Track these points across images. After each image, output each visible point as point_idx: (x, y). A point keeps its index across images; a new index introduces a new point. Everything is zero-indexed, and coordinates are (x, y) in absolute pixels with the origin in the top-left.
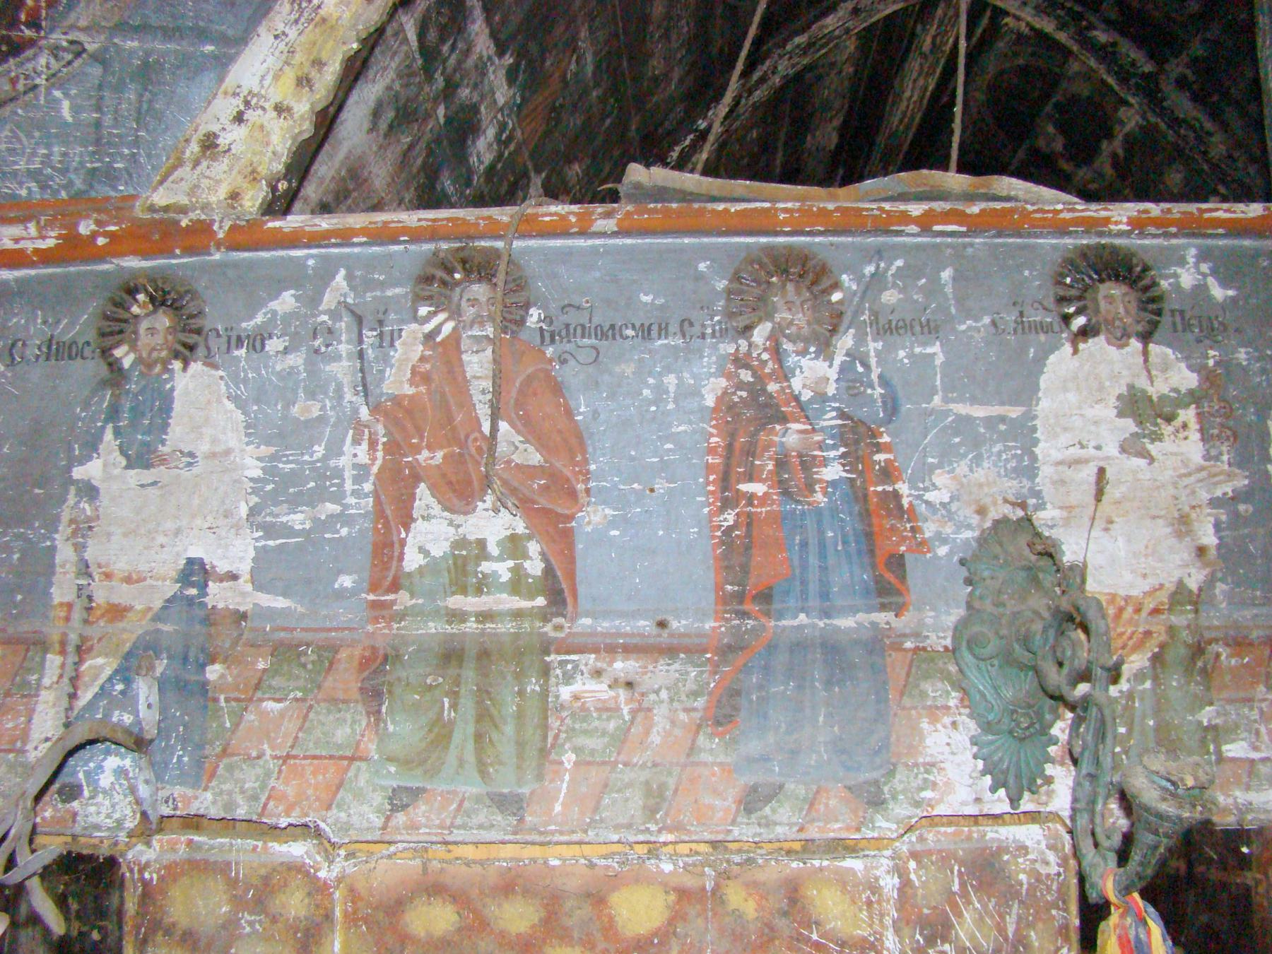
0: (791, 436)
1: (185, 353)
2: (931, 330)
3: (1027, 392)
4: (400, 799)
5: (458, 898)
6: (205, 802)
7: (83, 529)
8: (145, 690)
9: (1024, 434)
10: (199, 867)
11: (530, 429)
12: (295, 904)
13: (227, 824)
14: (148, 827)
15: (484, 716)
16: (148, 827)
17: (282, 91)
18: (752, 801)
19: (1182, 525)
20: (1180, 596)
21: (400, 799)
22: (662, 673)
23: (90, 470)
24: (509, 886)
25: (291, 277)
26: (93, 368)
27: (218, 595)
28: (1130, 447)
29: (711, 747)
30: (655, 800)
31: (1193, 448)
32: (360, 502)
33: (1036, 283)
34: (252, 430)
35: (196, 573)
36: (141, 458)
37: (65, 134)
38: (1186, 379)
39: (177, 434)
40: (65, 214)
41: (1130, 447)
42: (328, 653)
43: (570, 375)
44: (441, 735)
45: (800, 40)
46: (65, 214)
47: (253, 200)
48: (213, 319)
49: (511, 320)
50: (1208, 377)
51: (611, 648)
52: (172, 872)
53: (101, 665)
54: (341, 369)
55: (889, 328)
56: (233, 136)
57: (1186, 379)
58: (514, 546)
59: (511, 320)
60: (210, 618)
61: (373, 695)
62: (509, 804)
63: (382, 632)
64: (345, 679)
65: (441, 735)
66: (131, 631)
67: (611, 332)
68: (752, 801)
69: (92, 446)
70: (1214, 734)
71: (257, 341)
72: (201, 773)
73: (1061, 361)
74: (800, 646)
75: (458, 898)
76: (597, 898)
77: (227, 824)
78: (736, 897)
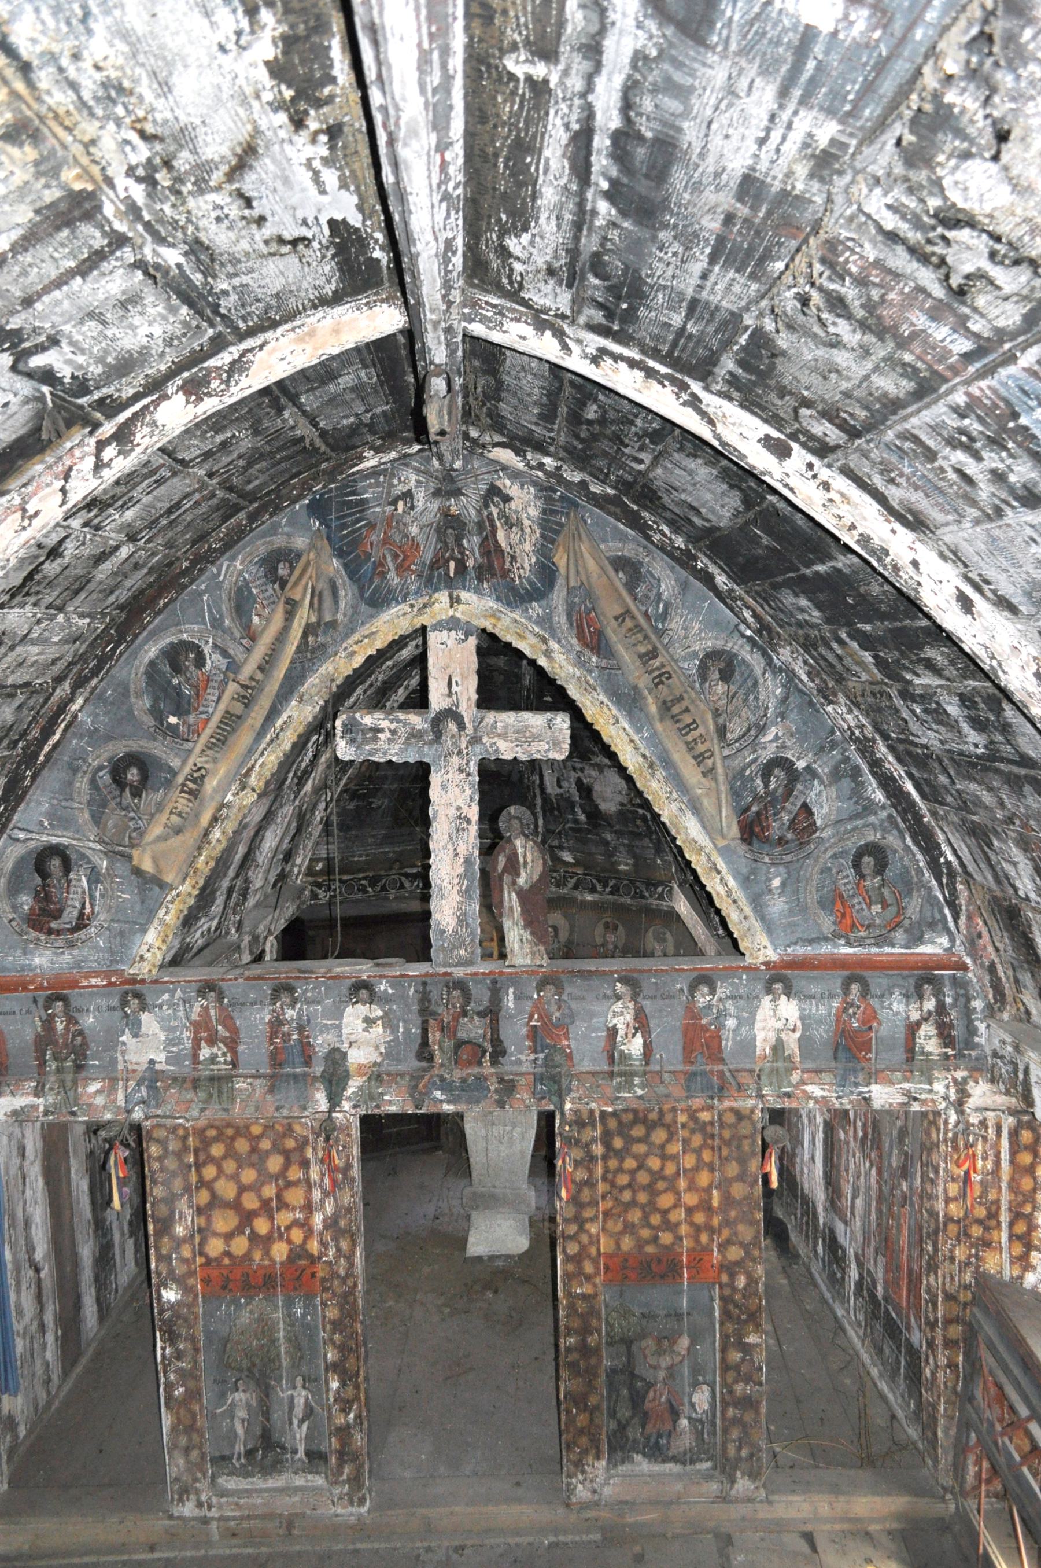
0: (285, 1028)
1: (143, 1010)
2: (318, 1003)
3: (340, 1017)
4: (202, 1110)
5: (217, 1128)
6: (159, 1112)
7: (123, 1052)
8: (143, 1089)
9: (339, 1027)
10: (159, 1126)
11: (225, 1026)
12: (181, 1132)
13: (164, 1117)
14: (147, 1118)
15: (220, 1092)
16: (147, 1118)
17: (158, 944)
18: (278, 1109)
19: (377, 1048)
20: (375, 1064)
21: (202, 1110)
22: (258, 1082)
23: (123, 1038)
24: (228, 1125)
25: (168, 991)
26: (118, 1014)
27: (158, 1067)
28: (365, 1030)
29: (269, 1097)
30: (257, 1109)
31: (380, 1030)
32: (188, 1045)
33: (345, 991)
34: (162, 1028)
35: (152, 1062)
36: (136, 1035)
37: (102, 950)
38: (380, 1013)
39: (144, 1030)
40: (107, 974)
41: (365, 1030)
42: (184, 1080)
43: (234, 1014)
44: (211, 1095)
45: (389, 663)
46: (107, 974)
47: (154, 971)
48: (149, 1001)
49: (220, 998)
50: (386, 1013)
51: (246, 1077)
52: (153, 1127)
53: (132, 1084)
54: (181, 1014)
55: (309, 1002)
56: (148, 955)
57: (380, 1013)
58: (224, 1055)
59: (220, 998)
60: (157, 1072)
61: (195, 1088)
62: (226, 1110)
63: (196, 1074)
64: (188, 1085)
65: (211, 1095)
66: (138, 1075)
67: (243, 1004)
68: (278, 1109)
69: (123, 1033)
70: (382, 1094)
71: (160, 1006)
72: (158, 1106)
73: (349, 1010)
74: (288, 1075)
75: (217, 1128)
76: (247, 1127)
77: (164, 1117)
78: (278, 1127)
